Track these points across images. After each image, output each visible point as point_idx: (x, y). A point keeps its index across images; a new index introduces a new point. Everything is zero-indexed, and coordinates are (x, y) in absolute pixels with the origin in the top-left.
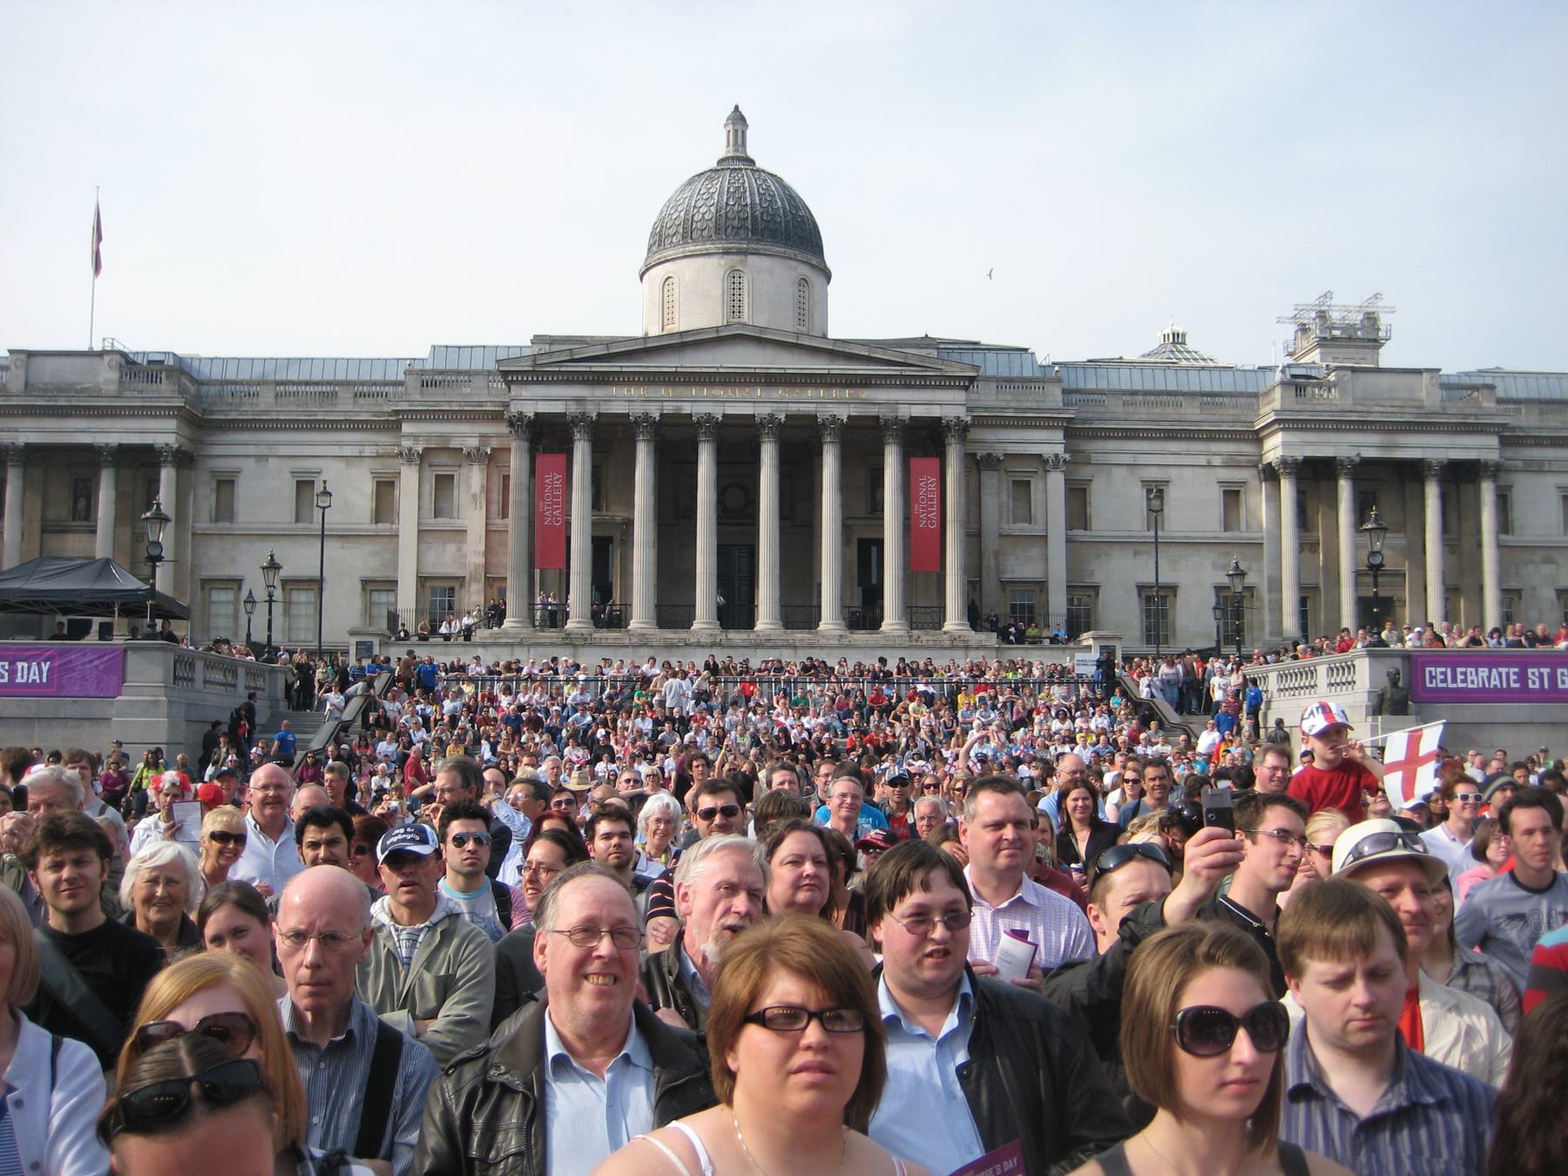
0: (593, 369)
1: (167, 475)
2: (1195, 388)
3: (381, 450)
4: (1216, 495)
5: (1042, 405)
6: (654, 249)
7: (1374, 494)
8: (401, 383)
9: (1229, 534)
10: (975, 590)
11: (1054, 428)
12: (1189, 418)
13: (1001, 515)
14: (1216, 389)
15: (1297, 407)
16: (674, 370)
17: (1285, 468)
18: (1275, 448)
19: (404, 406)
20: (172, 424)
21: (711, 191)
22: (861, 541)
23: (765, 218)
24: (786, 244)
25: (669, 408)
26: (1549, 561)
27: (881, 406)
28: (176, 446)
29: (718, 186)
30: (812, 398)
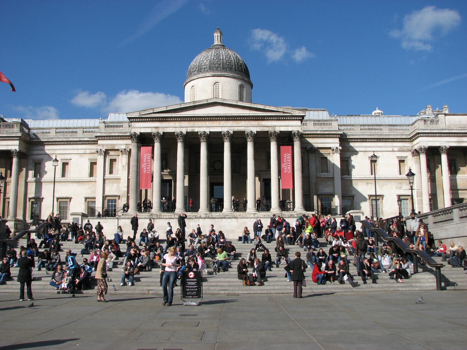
2: (387, 123)
3: (92, 151)
7: (454, 160)
8: (98, 128)
9: (401, 176)
10: (307, 198)
11: (335, 137)
12: (385, 134)
14: (394, 123)
15: (424, 128)
17: (421, 151)
19: (99, 135)
21: (208, 55)
23: (227, 63)
24: (235, 73)
25: (189, 130)
29: (210, 54)
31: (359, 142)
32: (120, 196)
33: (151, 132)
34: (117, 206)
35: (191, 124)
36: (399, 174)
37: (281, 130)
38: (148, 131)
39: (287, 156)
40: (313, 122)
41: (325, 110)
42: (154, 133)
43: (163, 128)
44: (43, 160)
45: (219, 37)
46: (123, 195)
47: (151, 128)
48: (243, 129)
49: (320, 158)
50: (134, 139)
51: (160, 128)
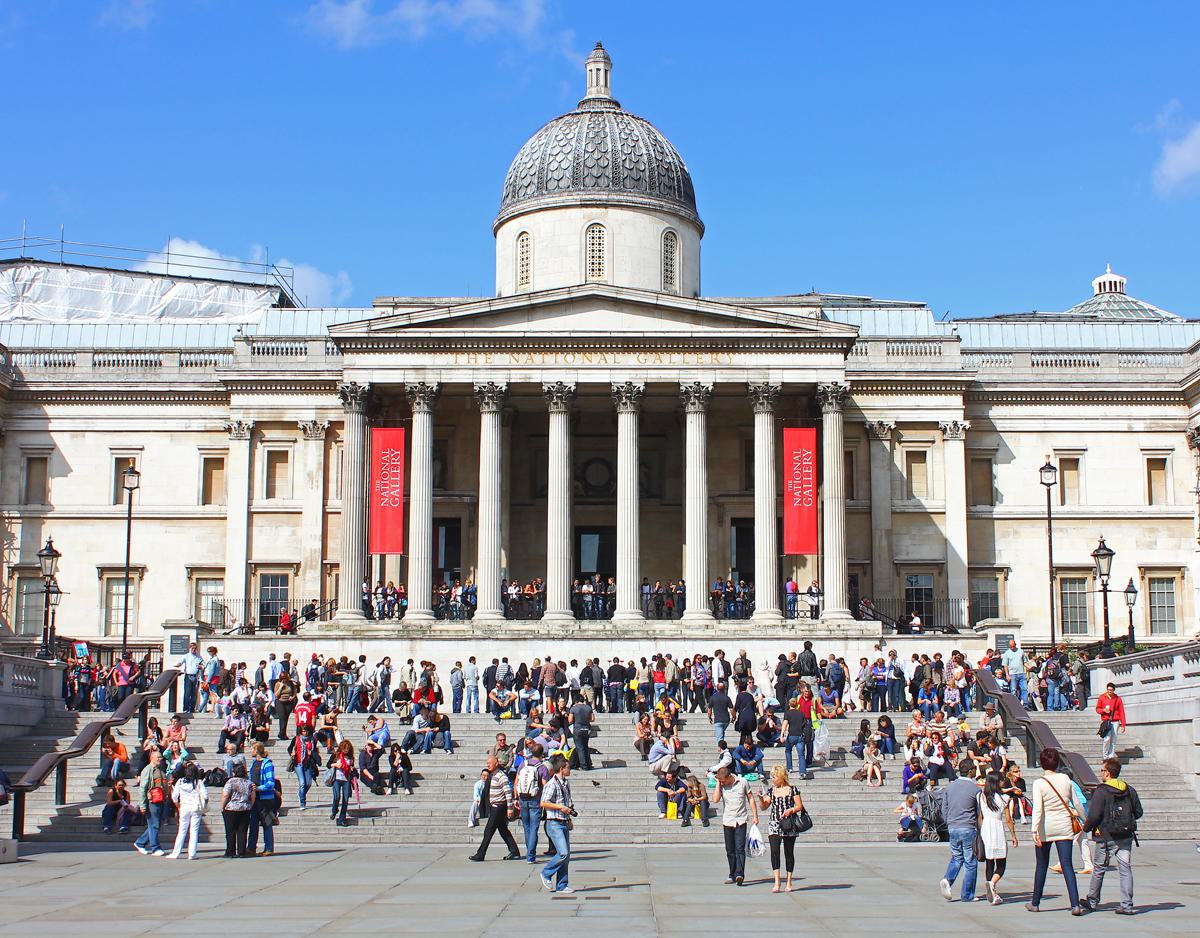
0: (433, 335)
2: (1115, 345)
3: (210, 425)
5: (938, 368)
6: (508, 201)
8: (228, 351)
10: (865, 573)
11: (951, 393)
12: (1106, 378)
16: (522, 335)
21: (569, 137)
24: (651, 194)
25: (517, 377)
27: (750, 372)
29: (576, 132)
32: (298, 565)
34: (290, 597)
35: (523, 359)
36: (1147, 503)
40: (884, 346)
41: (923, 306)
42: (411, 385)
43: (438, 372)
44: (53, 449)
45: (602, 73)
46: (309, 563)
47: (402, 371)
48: (673, 376)
50: (350, 404)
51: (430, 372)
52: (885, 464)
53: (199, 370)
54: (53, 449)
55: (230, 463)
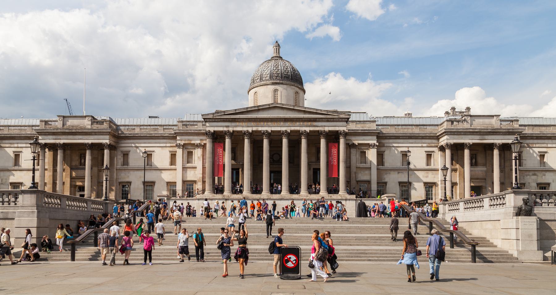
1: (106, 152)
4: (424, 155)
5: (370, 129)
6: (252, 84)
7: (476, 154)
9: (428, 167)
11: (373, 135)
13: (356, 161)
18: (444, 141)
20: (108, 137)
22: (314, 169)
23: (285, 73)
25: (255, 129)
26: (535, 175)
28: (109, 143)
29: (271, 64)
30: (298, 125)
31: (393, 139)
33: (223, 130)
37: (330, 130)
38: (221, 129)
39: (334, 151)
44: (130, 151)
49: (360, 152)
52: (355, 154)
53: (169, 130)
54: (130, 151)
55: (177, 154)
